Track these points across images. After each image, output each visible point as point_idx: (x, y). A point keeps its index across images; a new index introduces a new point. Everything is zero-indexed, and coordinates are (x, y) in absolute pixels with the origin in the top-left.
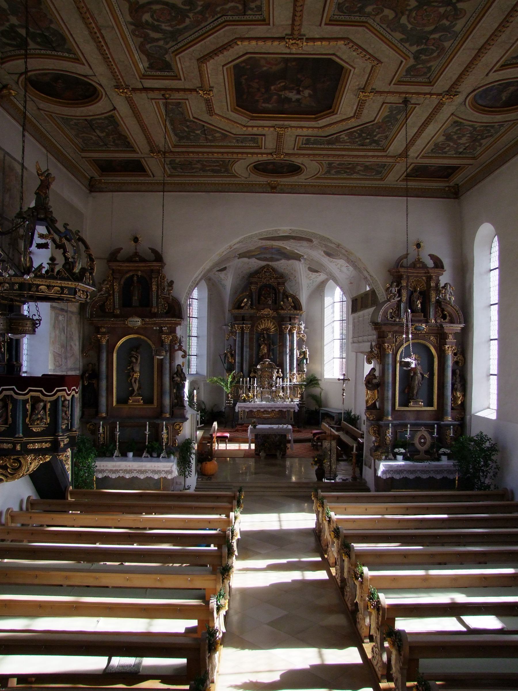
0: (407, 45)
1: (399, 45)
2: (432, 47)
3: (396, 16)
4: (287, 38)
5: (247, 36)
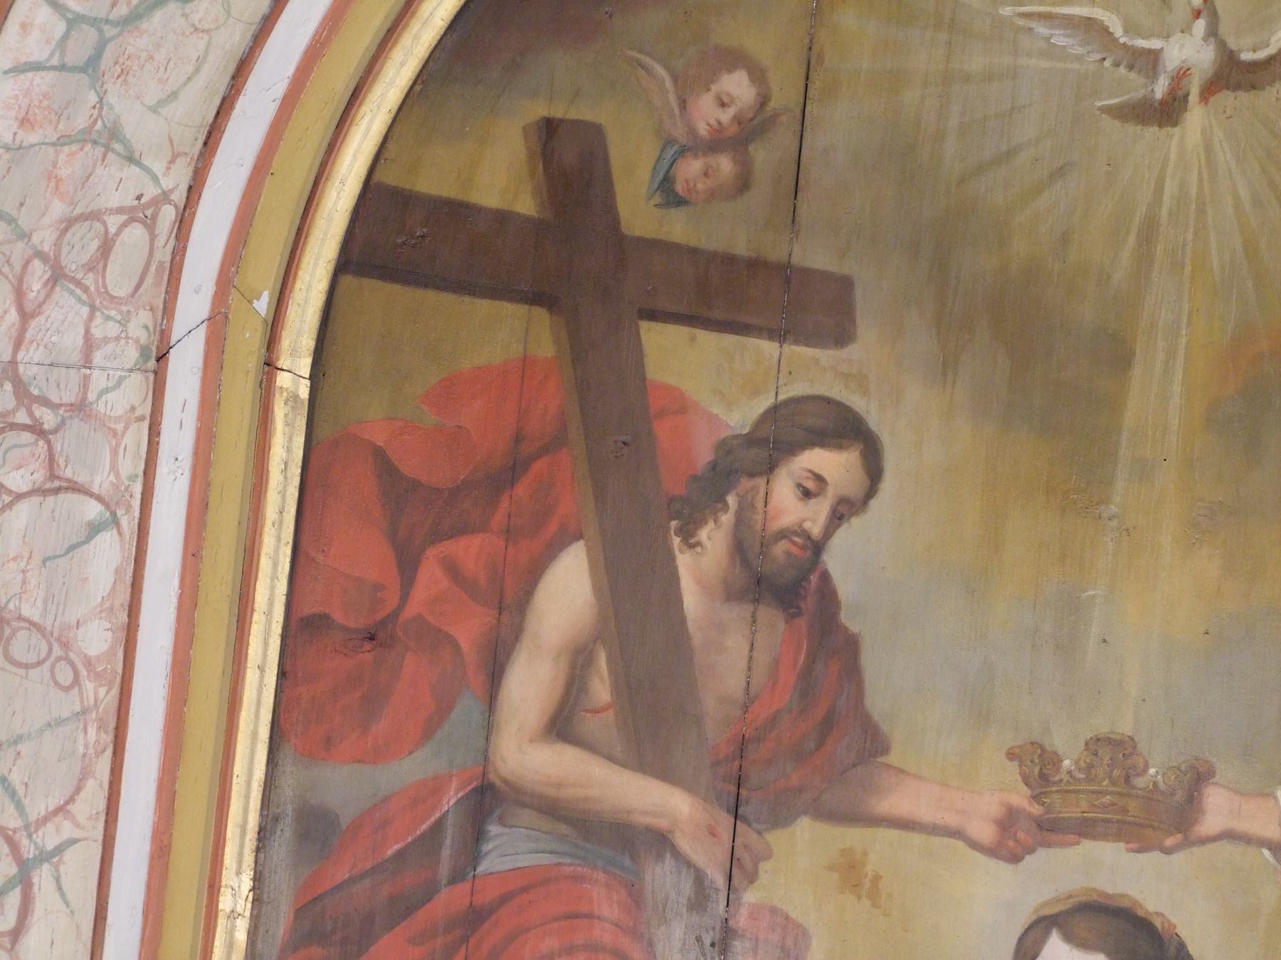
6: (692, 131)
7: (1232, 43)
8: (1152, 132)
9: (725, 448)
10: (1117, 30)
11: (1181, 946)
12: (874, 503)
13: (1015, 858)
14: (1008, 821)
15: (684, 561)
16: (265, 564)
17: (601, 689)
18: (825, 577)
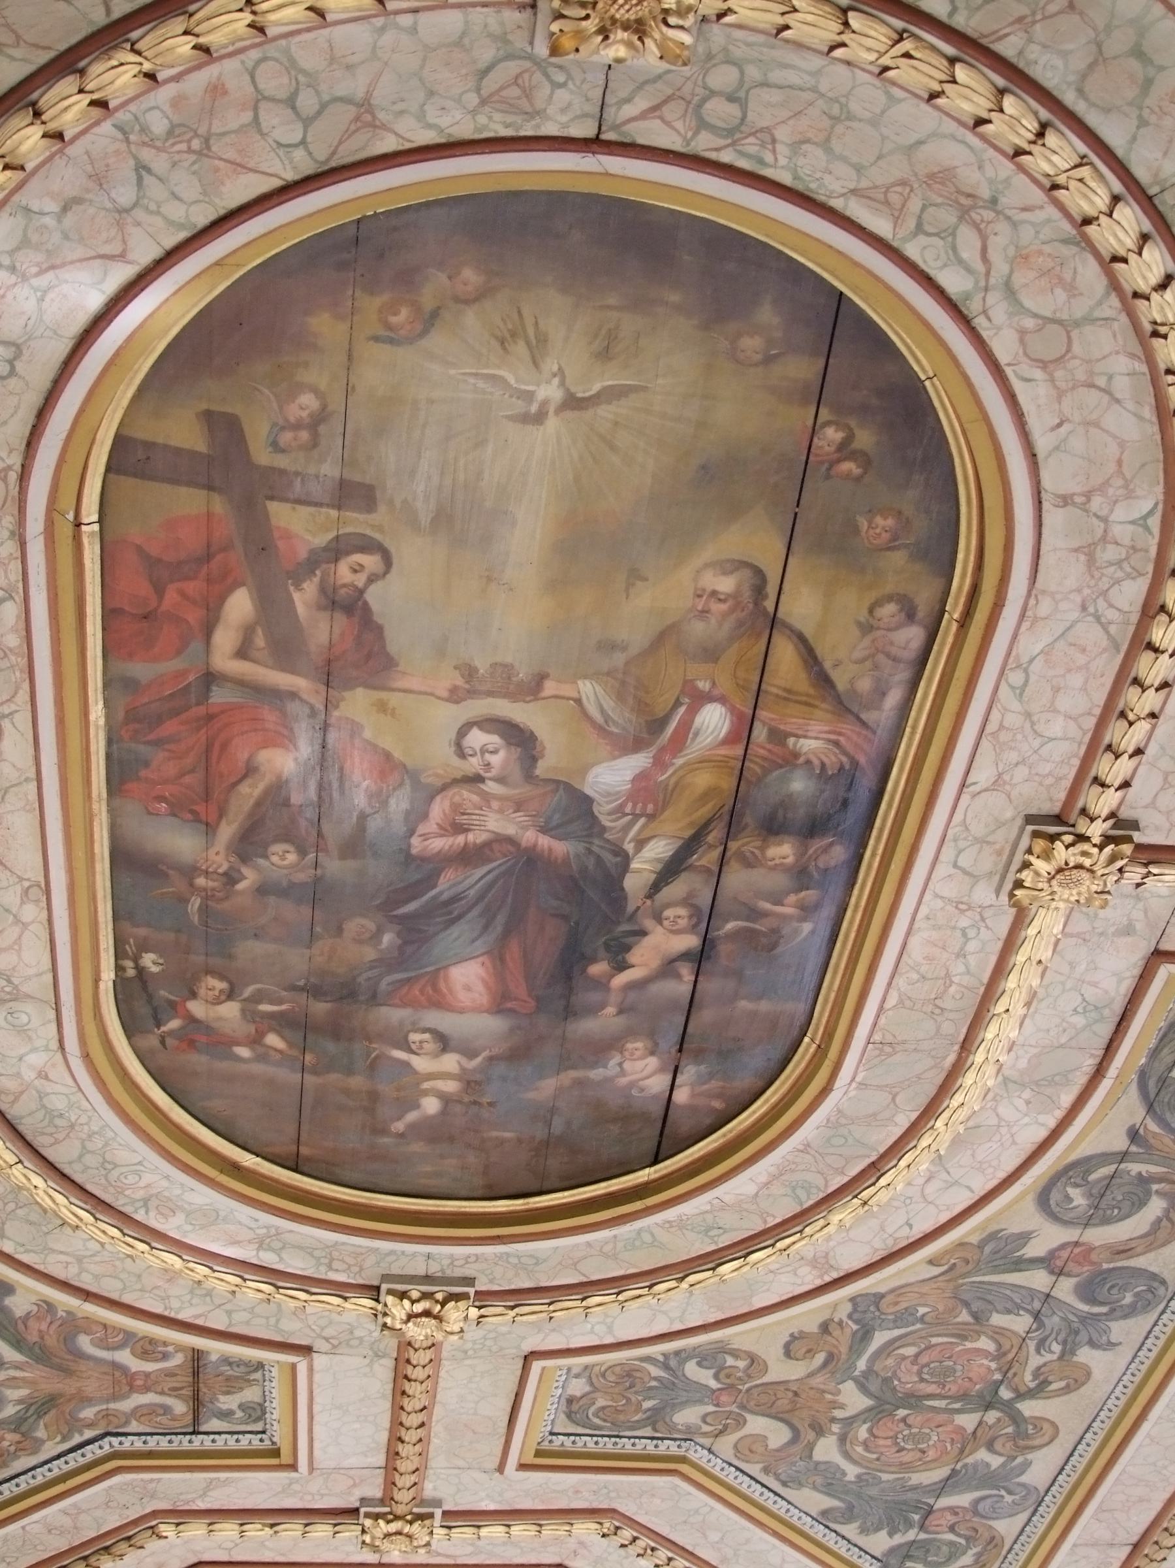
0: (850, 1530)
1: (819, 1532)
2: (951, 1537)
3: (796, 1436)
4: (367, 1515)
5: (201, 1505)
6: (287, 420)
7: (573, 390)
8: (529, 428)
9: (313, 552)
10: (512, 380)
11: (532, 733)
12: (388, 576)
13: (457, 702)
14: (454, 690)
15: (296, 596)
16: (89, 599)
17: (260, 641)
18: (366, 603)
